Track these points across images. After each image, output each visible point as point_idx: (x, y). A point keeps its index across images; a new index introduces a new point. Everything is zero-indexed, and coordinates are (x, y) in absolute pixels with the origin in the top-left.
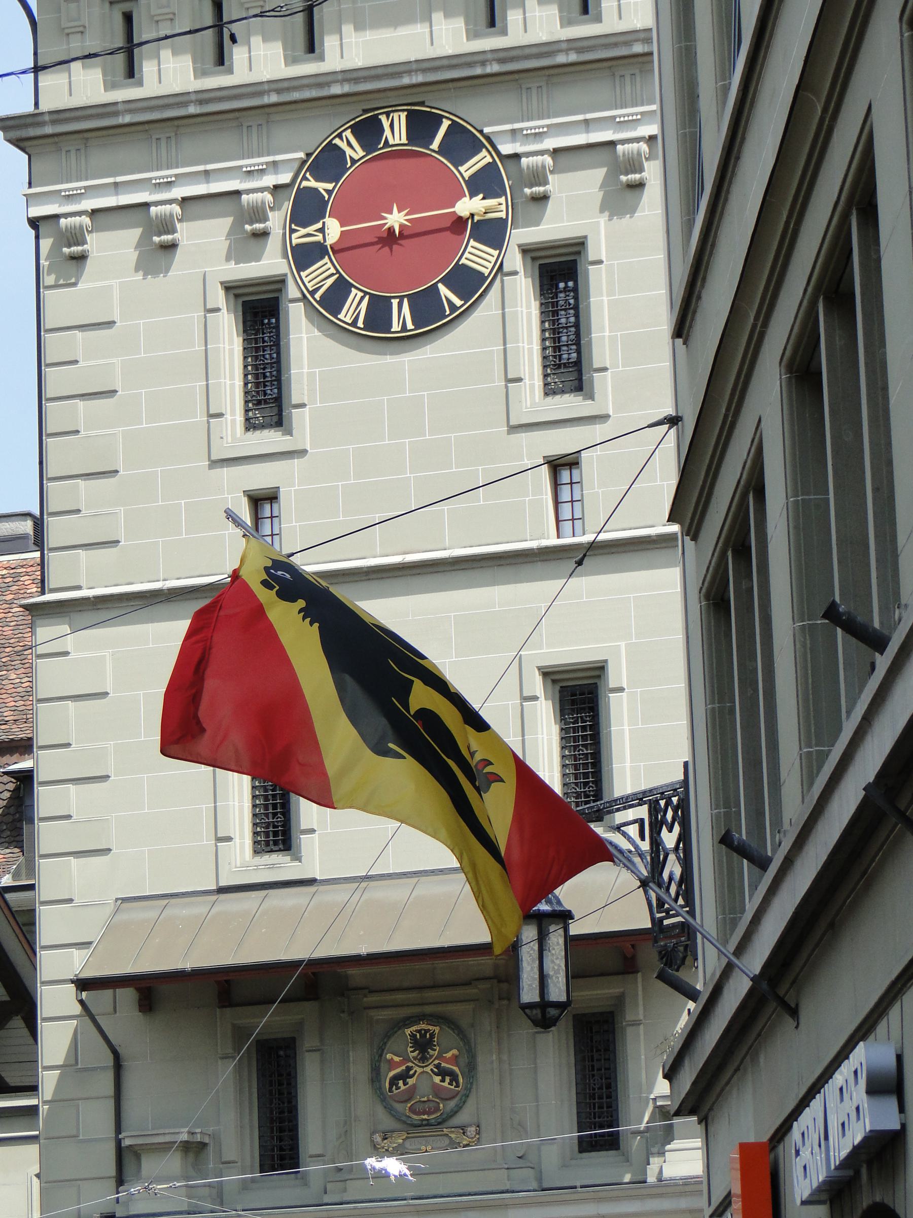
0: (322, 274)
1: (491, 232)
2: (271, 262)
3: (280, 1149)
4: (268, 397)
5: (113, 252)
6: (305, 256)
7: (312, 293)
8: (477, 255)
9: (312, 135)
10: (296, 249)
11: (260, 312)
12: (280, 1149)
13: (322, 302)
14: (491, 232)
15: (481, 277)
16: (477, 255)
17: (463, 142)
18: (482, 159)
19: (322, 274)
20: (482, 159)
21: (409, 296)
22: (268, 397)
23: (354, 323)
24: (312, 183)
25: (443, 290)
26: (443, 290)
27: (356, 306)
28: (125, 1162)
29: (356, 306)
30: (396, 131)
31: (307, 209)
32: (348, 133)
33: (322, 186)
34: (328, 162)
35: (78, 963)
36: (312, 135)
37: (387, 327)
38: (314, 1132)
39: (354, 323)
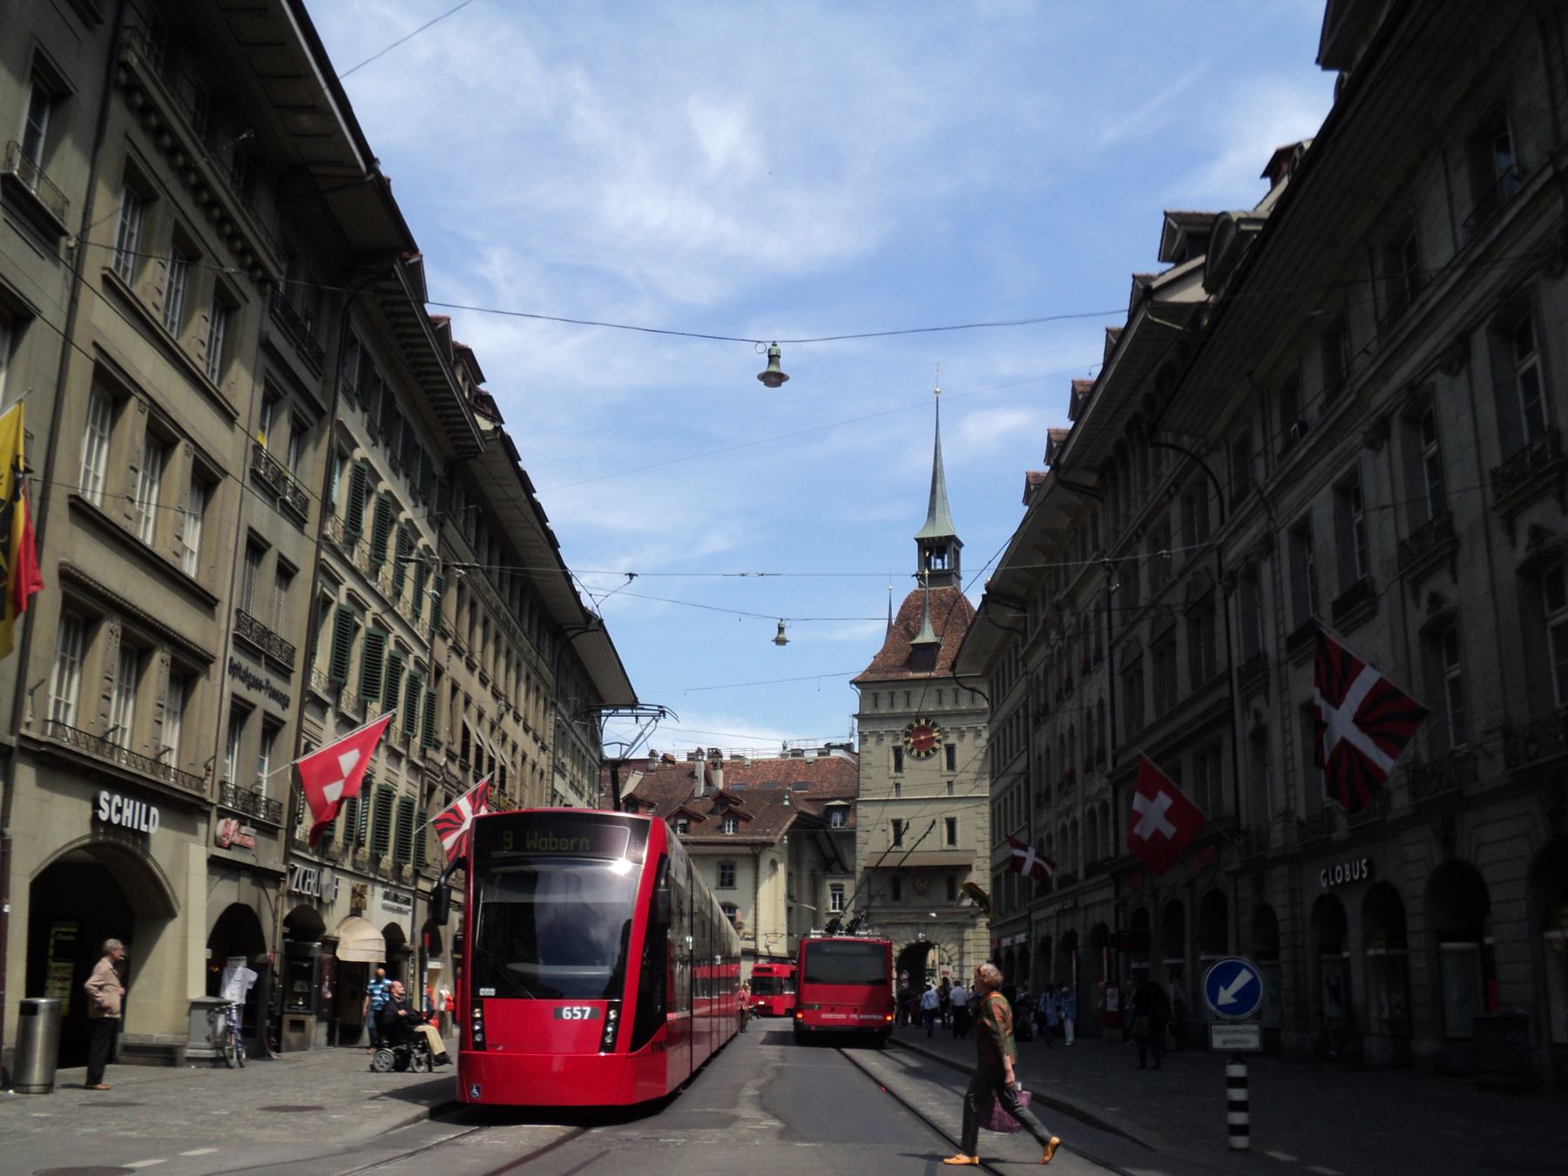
2: (900, 743)
3: (897, 896)
4: (899, 766)
5: (872, 741)
8: (936, 745)
9: (908, 722)
11: (898, 752)
12: (897, 896)
16: (936, 745)
17: (934, 725)
21: (925, 749)
22: (899, 766)
27: (915, 752)
28: (871, 898)
29: (915, 752)
30: (923, 722)
31: (907, 734)
34: (911, 727)
35: (864, 864)
36: (908, 722)
38: (903, 894)
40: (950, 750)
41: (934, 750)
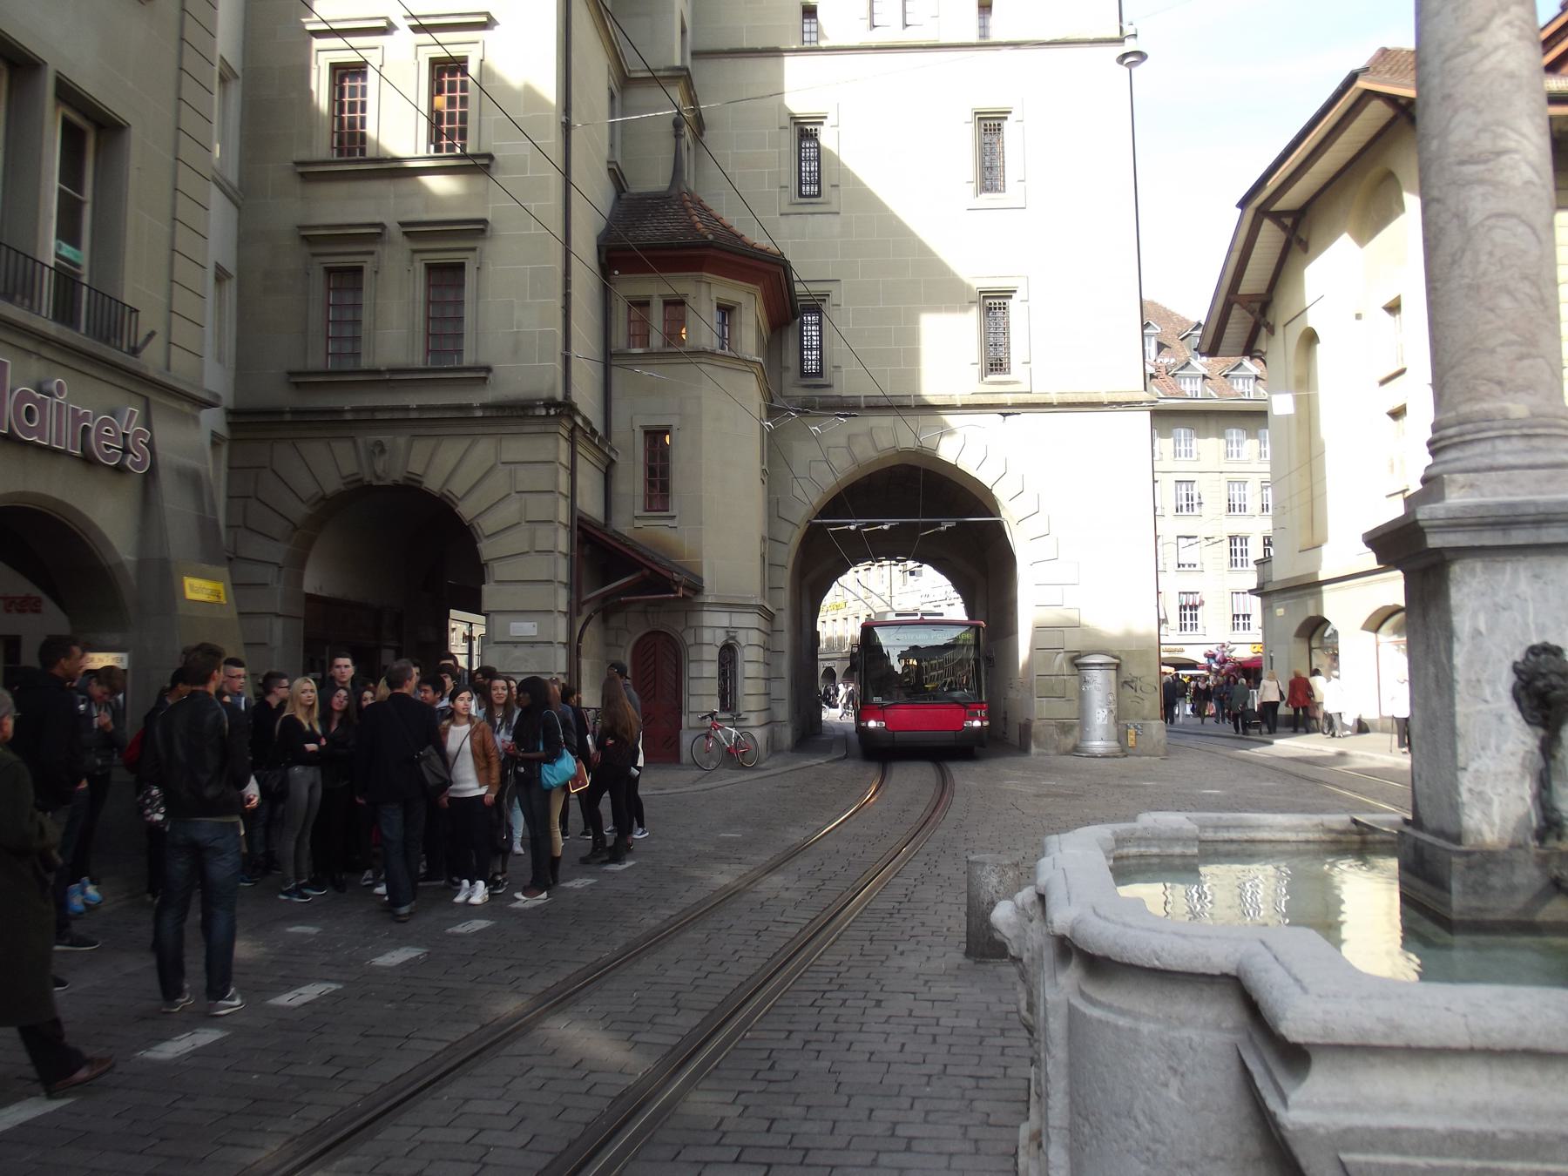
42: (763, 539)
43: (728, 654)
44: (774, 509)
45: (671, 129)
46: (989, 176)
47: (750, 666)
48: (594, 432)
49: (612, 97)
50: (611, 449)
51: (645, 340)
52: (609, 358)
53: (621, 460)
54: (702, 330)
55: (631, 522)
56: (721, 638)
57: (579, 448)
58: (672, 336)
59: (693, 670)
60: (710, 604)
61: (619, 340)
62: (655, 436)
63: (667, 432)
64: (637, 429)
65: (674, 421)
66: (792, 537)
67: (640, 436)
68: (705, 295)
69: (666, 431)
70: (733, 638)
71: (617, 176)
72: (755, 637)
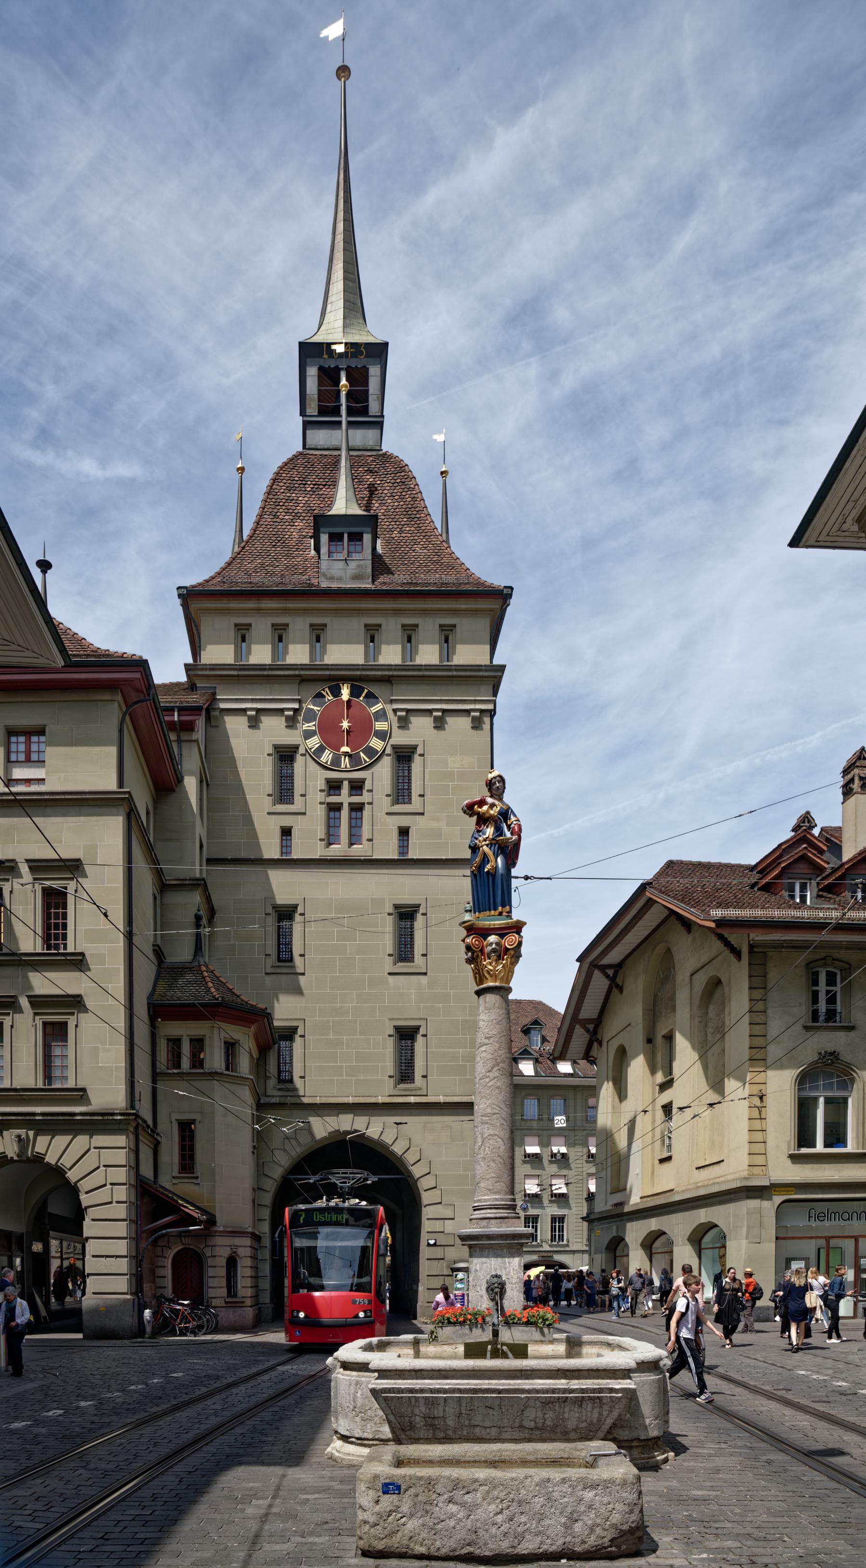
0: (314, 742)
1: (382, 735)
6: (308, 735)
7: (310, 749)
8: (376, 744)
10: (305, 732)
13: (314, 753)
14: (382, 735)
15: (377, 752)
18: (378, 707)
19: (314, 742)
20: (378, 707)
23: (326, 763)
24: (312, 707)
25: (362, 755)
26: (362, 755)
27: (327, 757)
32: (327, 689)
33: (315, 708)
37: (340, 766)
39: (326, 763)
40: (404, 756)
41: (370, 752)
42: (254, 1190)
43: (232, 1263)
44: (260, 1171)
45: (193, 919)
46: (404, 950)
47: (244, 1271)
48: (148, 1126)
49: (155, 898)
50: (158, 1134)
51: (178, 1066)
52: (155, 1076)
53: (163, 1141)
54: (215, 1059)
55: (169, 1180)
56: (226, 1252)
57: (141, 1137)
58: (197, 1062)
59: (211, 1272)
60: (220, 1232)
61: (162, 1066)
62: (186, 1129)
63: (193, 1123)
64: (174, 1121)
65: (197, 1117)
66: (271, 1186)
67: (175, 1126)
68: (216, 1035)
69: (193, 1122)
70: (235, 1252)
71: (158, 953)
72: (248, 1252)
